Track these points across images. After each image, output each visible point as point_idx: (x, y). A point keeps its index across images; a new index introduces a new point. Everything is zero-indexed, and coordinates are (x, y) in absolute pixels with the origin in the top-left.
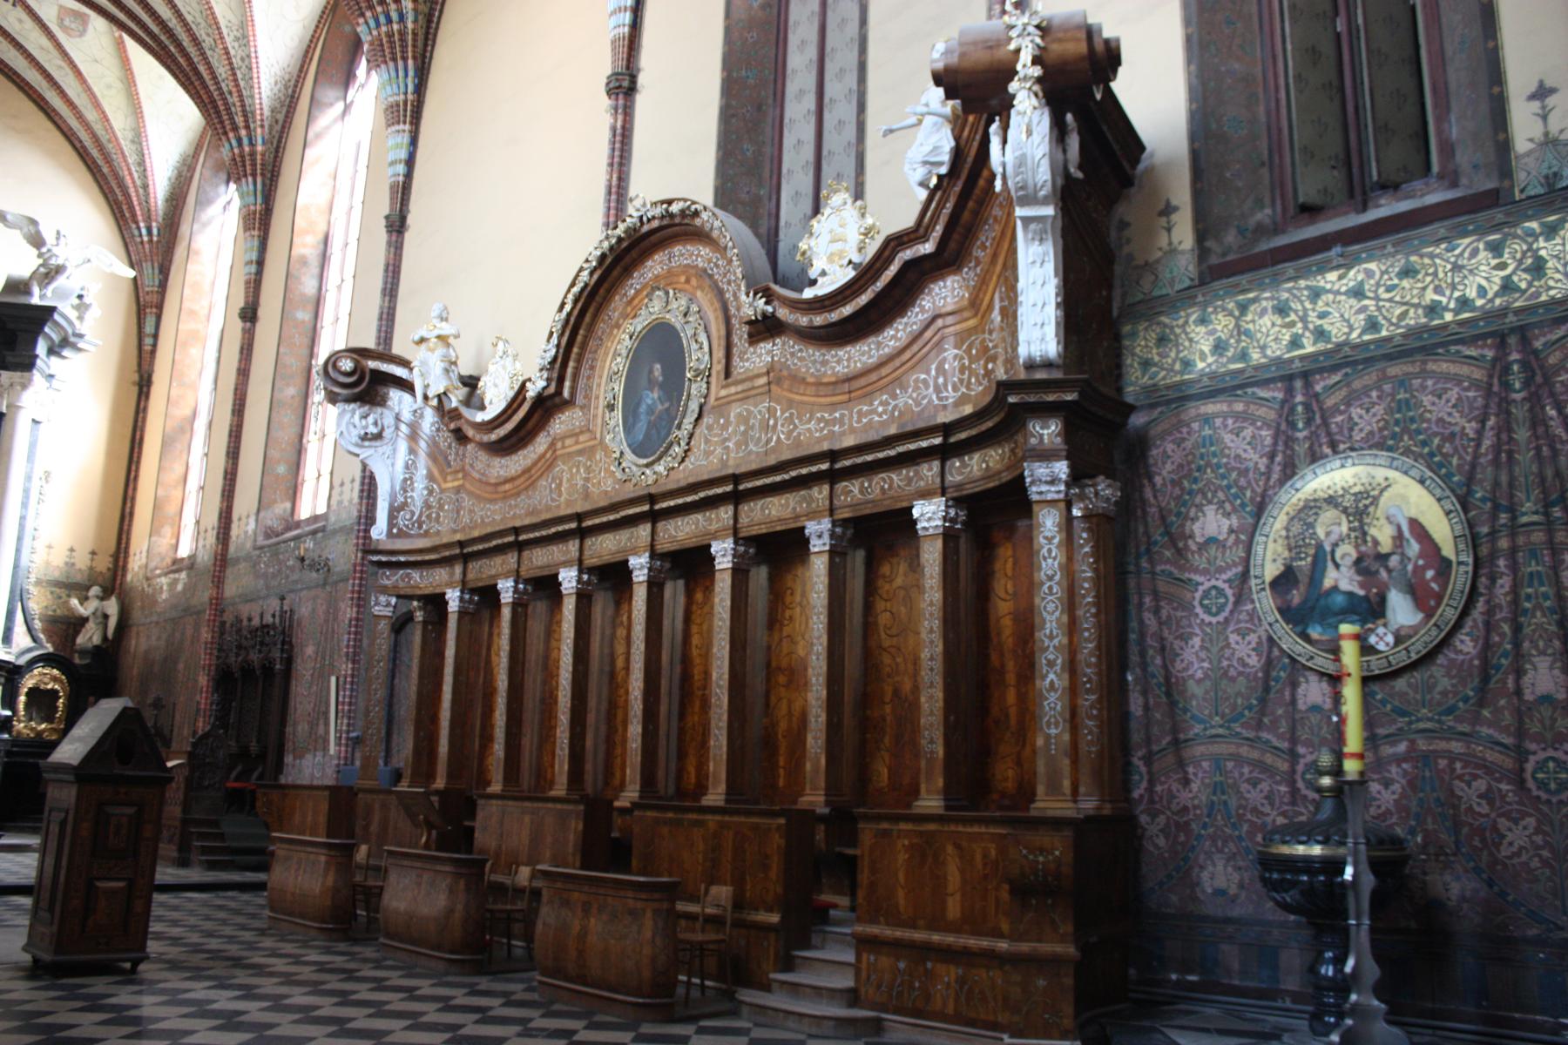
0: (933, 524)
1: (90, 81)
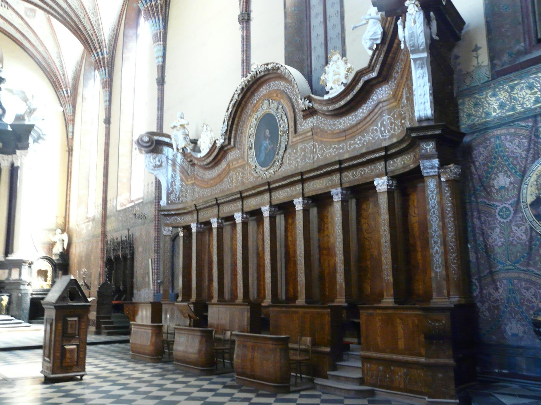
0: (383, 187)
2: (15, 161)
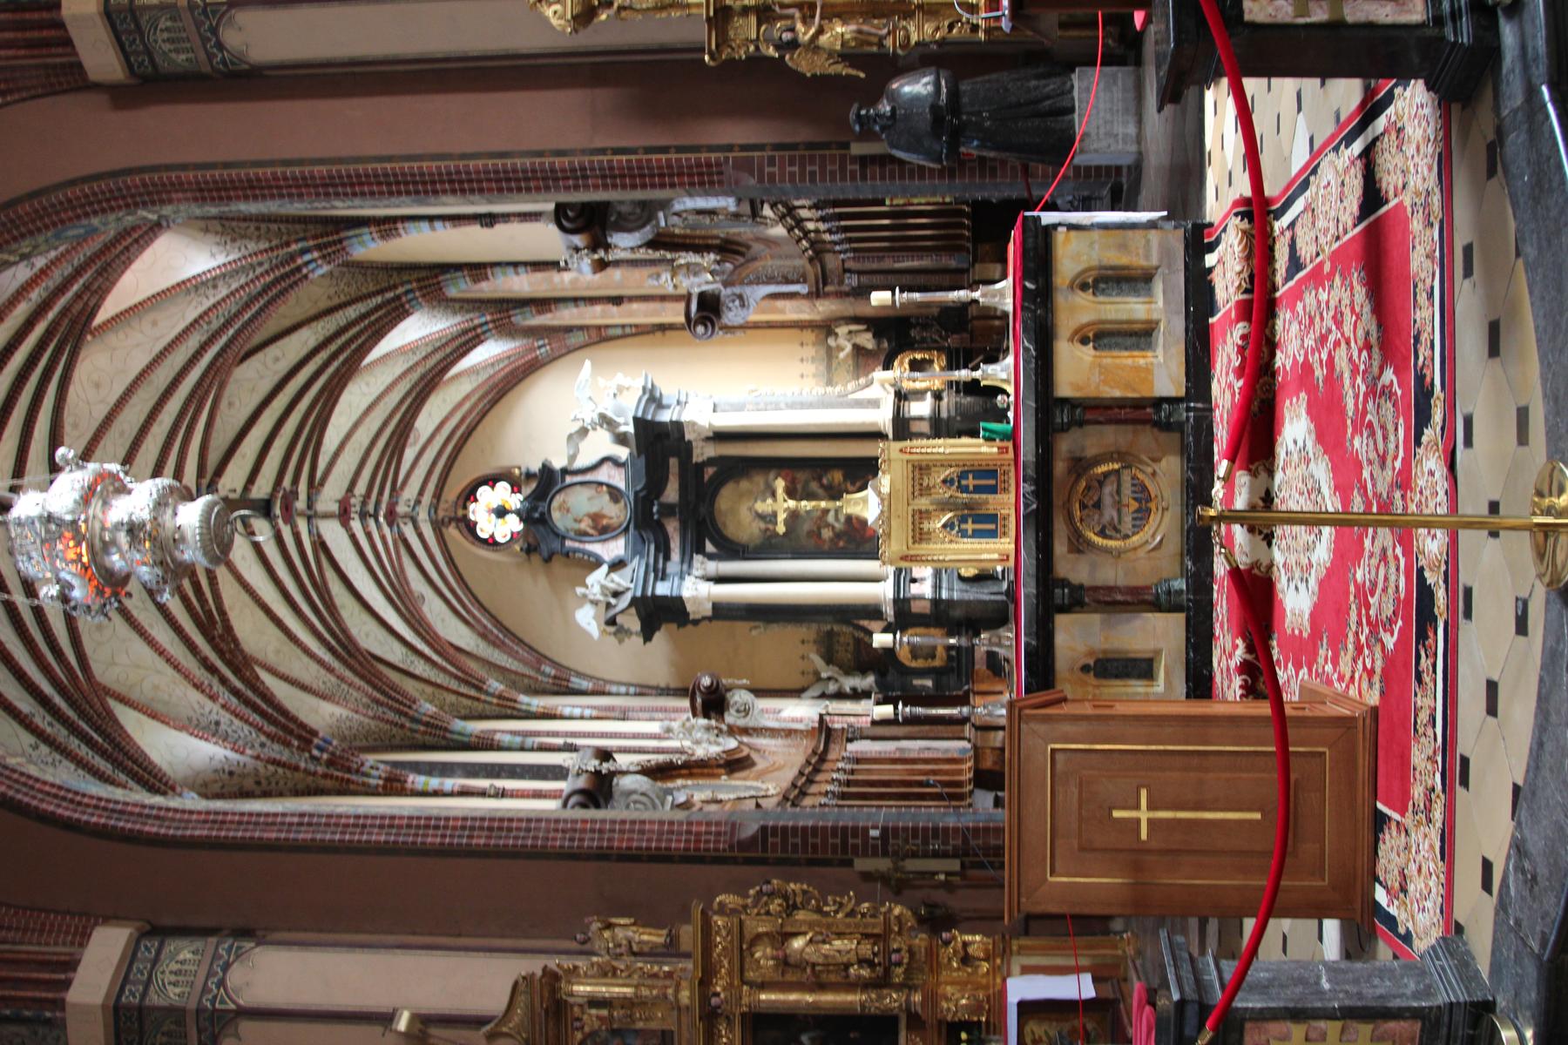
1: (444, 414)
2: (703, 436)
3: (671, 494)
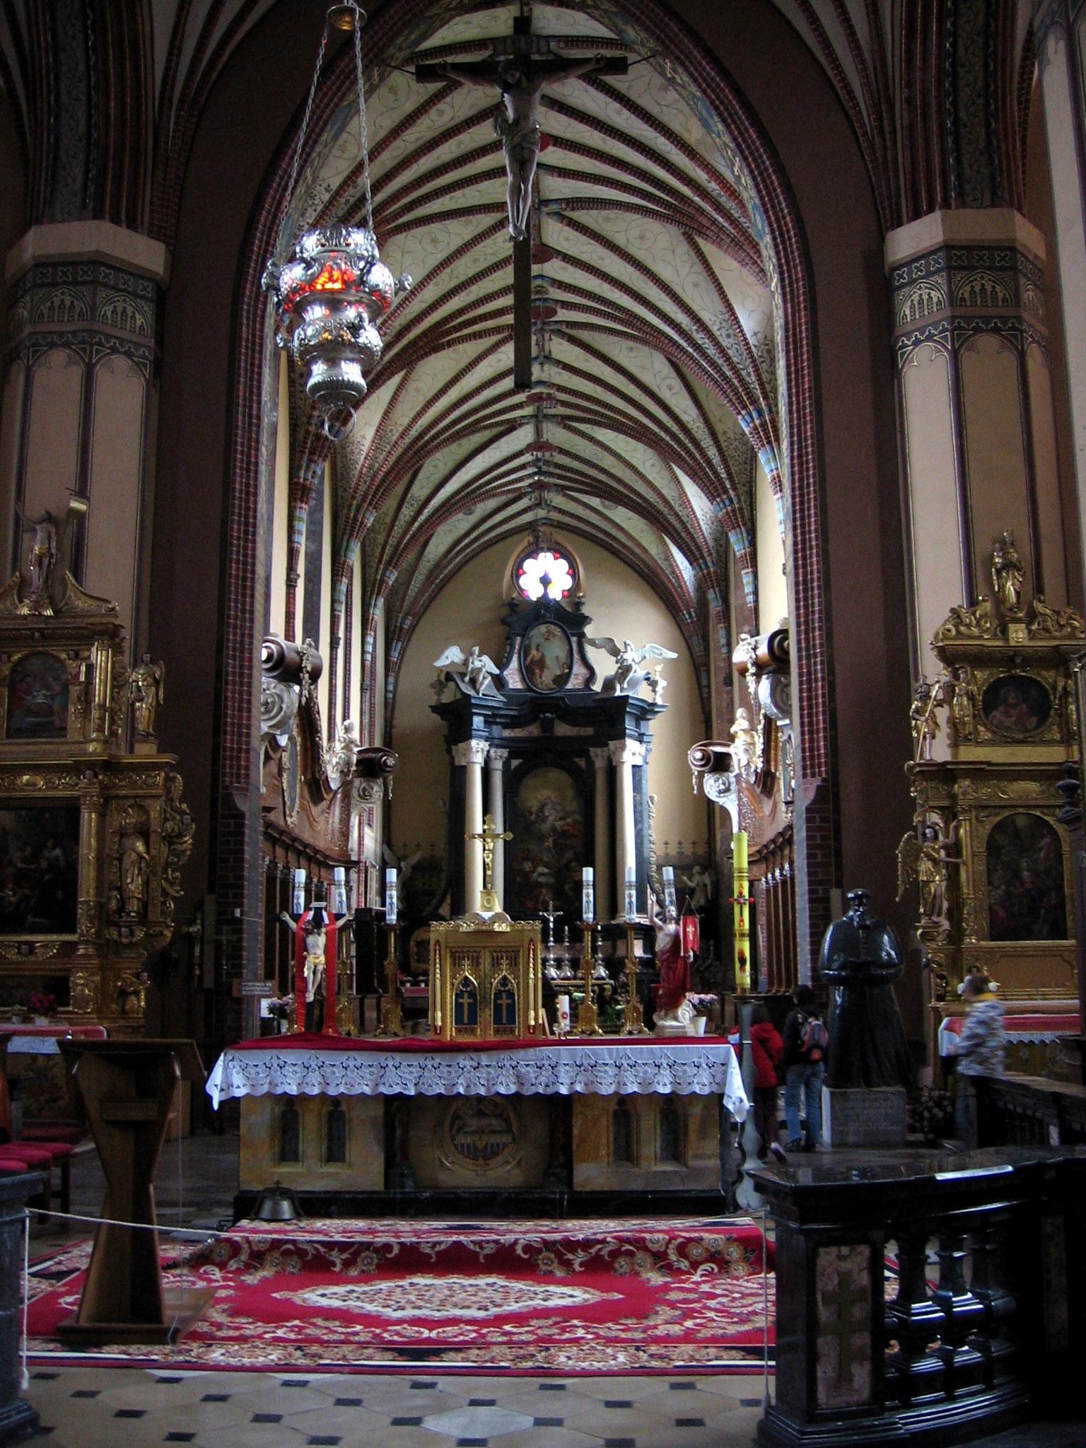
1: (630, 531)
3: (562, 729)
